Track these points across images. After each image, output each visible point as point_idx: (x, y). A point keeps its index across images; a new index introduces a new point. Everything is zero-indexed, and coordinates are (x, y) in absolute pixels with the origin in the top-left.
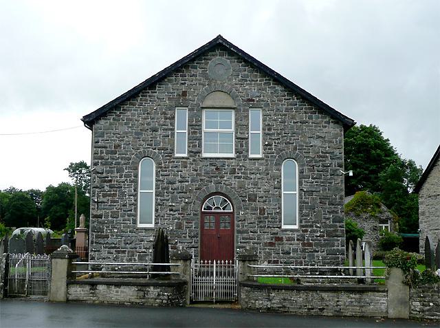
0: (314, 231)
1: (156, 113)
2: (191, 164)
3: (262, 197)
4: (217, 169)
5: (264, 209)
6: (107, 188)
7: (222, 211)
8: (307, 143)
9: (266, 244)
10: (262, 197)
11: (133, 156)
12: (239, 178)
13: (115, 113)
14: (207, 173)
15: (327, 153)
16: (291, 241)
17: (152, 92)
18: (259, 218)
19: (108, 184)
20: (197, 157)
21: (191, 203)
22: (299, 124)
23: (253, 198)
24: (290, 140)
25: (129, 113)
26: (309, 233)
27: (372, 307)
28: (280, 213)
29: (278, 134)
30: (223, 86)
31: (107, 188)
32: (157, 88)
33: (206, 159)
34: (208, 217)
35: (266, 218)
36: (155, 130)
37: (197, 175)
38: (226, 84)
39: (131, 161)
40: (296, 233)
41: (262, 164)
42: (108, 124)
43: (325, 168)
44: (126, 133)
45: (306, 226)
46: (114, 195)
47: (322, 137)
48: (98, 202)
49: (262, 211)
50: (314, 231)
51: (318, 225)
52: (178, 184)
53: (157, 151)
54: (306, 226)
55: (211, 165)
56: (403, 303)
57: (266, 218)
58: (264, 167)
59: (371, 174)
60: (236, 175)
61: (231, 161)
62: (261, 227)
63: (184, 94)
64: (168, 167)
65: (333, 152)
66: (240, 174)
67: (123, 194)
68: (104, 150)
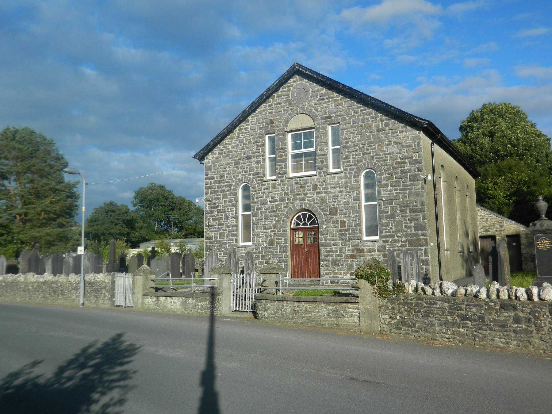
0: (395, 241)
1: (250, 143)
2: (280, 185)
3: (342, 210)
4: (301, 187)
5: (344, 222)
6: (215, 213)
7: (309, 226)
8: (385, 151)
9: (347, 256)
10: (342, 210)
11: (234, 183)
12: (320, 193)
13: (219, 148)
14: (292, 191)
15: (406, 158)
16: (372, 252)
17: (247, 125)
18: (341, 231)
19: (216, 210)
20: (284, 178)
21: (280, 221)
22: (376, 133)
23: (333, 212)
24: (367, 150)
25: (229, 147)
26: (390, 243)
27: (346, 319)
28: (360, 225)
29: (355, 146)
30: (304, 109)
31: (215, 213)
32: (250, 121)
33: (292, 178)
34: (297, 232)
35: (348, 230)
36: (249, 158)
37: (285, 194)
38: (306, 106)
39: (232, 188)
40: (376, 244)
41: (340, 178)
42: (214, 158)
43: (404, 174)
44: (228, 164)
45: (387, 236)
46: (221, 219)
47: (400, 143)
48: (209, 226)
49: (343, 223)
50: (395, 241)
51: (399, 235)
52: (269, 204)
53: (251, 177)
54: (387, 236)
55: (297, 183)
56: (371, 316)
57: (348, 230)
58: (343, 180)
59: (54, 218)
60: (318, 190)
61: (313, 177)
62: (343, 240)
63: (272, 122)
64: (261, 190)
65: (412, 157)
66: (322, 190)
67: (227, 217)
68: (213, 181)
